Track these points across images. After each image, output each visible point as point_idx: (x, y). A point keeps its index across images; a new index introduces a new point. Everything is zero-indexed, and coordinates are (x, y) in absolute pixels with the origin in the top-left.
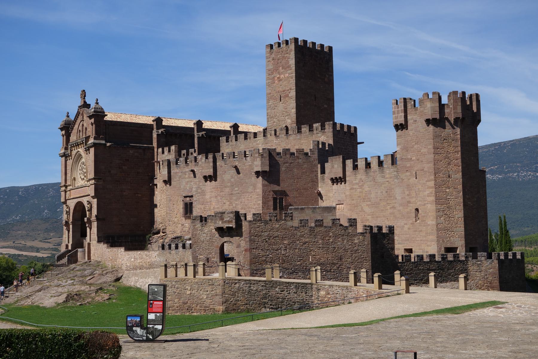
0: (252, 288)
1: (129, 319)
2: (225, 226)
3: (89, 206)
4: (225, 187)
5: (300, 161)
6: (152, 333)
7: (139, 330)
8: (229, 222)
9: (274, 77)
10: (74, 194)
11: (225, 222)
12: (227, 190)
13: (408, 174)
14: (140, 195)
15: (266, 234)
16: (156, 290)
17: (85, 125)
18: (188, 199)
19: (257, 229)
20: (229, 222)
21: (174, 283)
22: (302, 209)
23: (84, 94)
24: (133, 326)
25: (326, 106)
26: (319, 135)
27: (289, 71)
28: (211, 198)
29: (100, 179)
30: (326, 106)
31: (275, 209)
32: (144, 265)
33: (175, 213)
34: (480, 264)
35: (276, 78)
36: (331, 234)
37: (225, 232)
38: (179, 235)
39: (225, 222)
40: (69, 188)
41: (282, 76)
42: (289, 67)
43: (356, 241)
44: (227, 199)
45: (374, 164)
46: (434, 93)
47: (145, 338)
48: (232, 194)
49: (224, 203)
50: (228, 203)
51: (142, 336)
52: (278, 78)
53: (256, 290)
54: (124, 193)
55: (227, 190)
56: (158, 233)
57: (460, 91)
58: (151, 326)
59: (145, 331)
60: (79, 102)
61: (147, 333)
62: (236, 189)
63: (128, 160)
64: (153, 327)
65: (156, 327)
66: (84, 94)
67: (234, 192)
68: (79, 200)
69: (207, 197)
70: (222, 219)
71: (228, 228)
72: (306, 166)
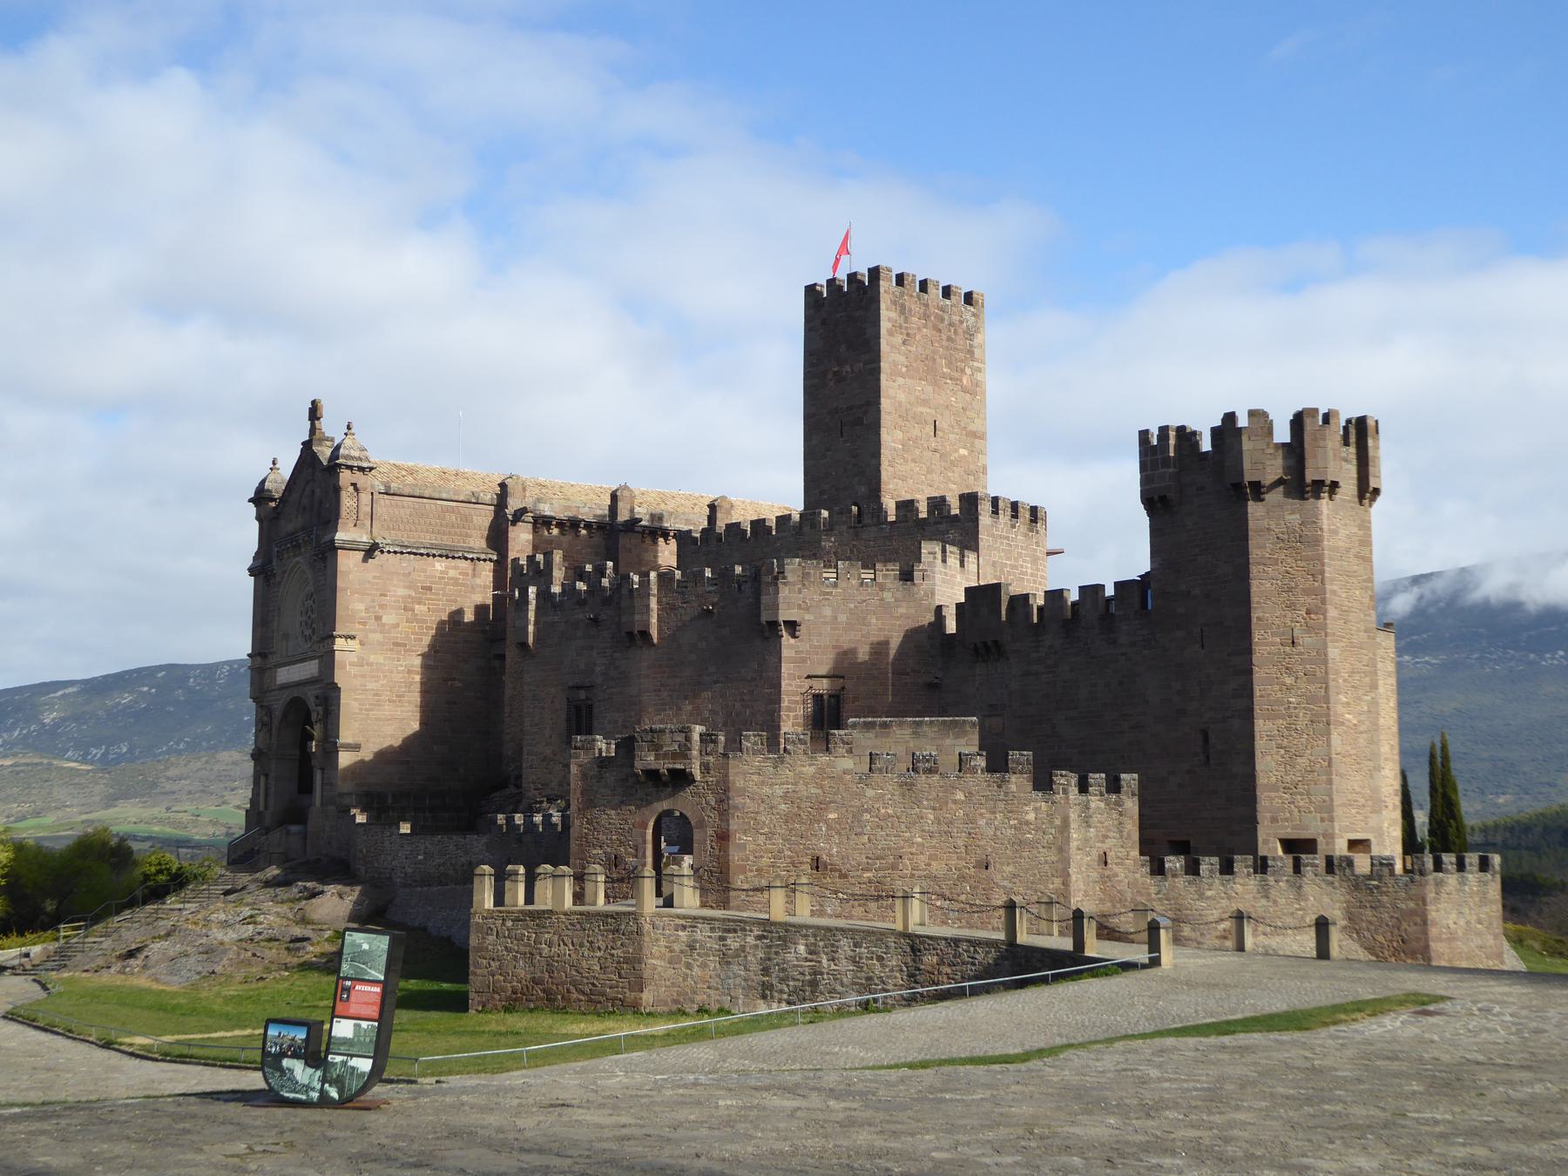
0: (729, 942)
1: (273, 1032)
2: (664, 766)
3: (320, 709)
5: (887, 596)
6: (338, 1082)
7: (299, 1070)
10: (285, 675)
11: (665, 755)
14: (458, 684)
15: (779, 791)
16: (366, 947)
17: (318, 491)
18: (582, 695)
19: (755, 778)
21: (509, 924)
22: (885, 725)
23: (314, 413)
24: (282, 1055)
25: (963, 452)
26: (943, 527)
29: (353, 638)
30: (963, 452)
34: (1377, 887)
35: (830, 376)
36: (960, 796)
37: (665, 785)
39: (665, 755)
40: (272, 660)
41: (848, 368)
43: (1031, 816)
46: (1252, 414)
47: (315, 1095)
51: (308, 1088)
53: (743, 948)
57: (1322, 411)
58: (338, 1059)
59: (319, 1073)
61: (324, 1080)
63: (430, 589)
64: (344, 1063)
65: (354, 1062)
66: (314, 413)
68: (296, 693)
70: (656, 748)
72: (902, 610)
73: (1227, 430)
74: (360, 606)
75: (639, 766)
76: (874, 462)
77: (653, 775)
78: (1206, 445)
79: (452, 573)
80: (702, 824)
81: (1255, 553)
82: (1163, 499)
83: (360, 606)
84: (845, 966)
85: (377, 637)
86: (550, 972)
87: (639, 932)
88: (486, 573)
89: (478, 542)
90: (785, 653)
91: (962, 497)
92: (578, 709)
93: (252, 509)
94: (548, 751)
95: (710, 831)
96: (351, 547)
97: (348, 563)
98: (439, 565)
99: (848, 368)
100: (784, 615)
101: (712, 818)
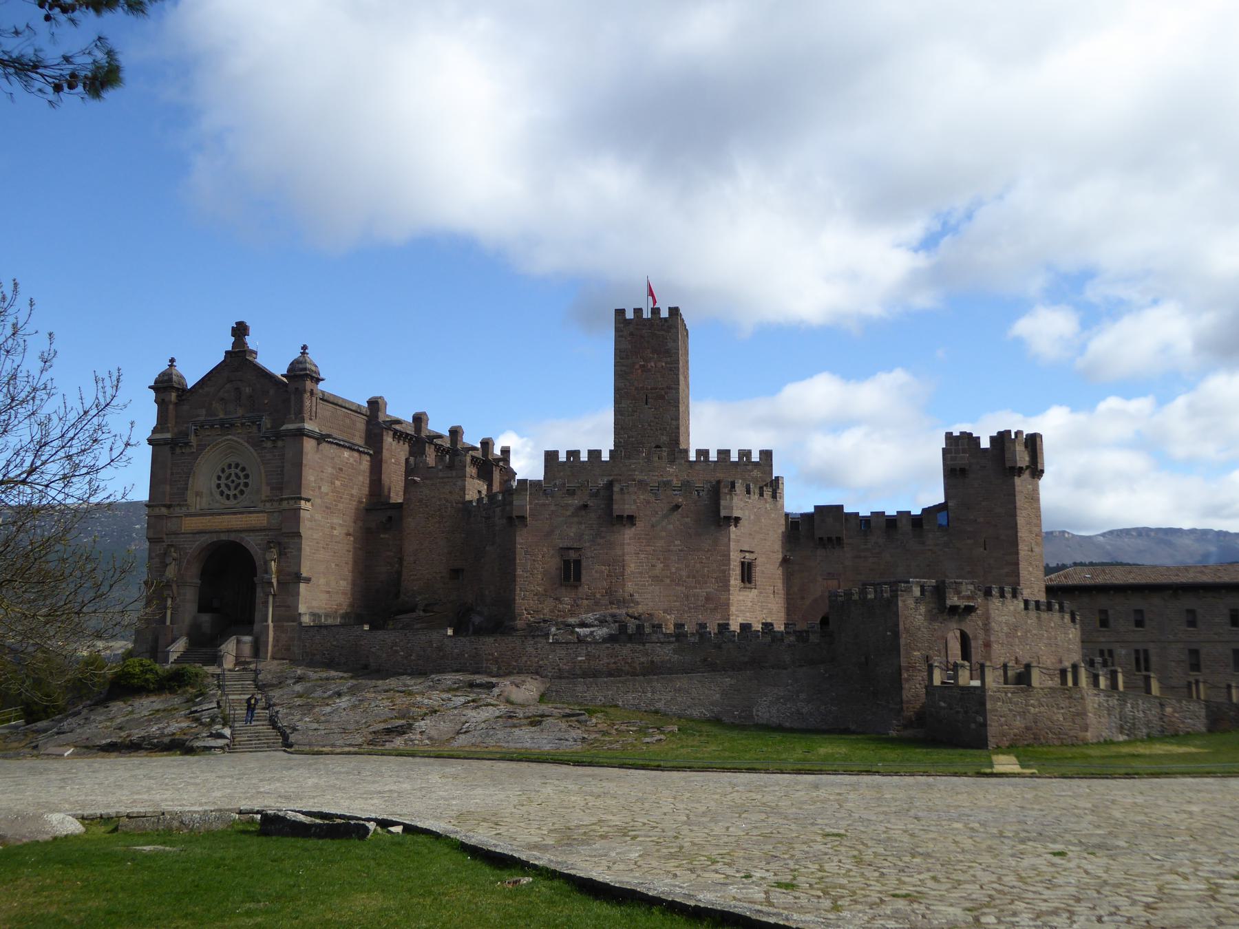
2: (963, 603)
8: (968, 598)
12: (660, 544)
13: (969, 541)
20: (968, 598)
26: (749, 467)
31: (743, 581)
32: (627, 668)
39: (963, 598)
45: (905, 526)
54: (335, 532)
55: (660, 543)
56: (413, 610)
60: (228, 343)
68: (224, 537)
70: (958, 593)
71: (966, 607)
73: (1001, 439)
74: (312, 479)
75: (949, 603)
76: (674, 423)
77: (954, 610)
78: (985, 443)
79: (351, 460)
80: (976, 638)
81: (1018, 504)
82: (963, 471)
83: (312, 479)
84: (1141, 715)
85: (318, 501)
86: (1035, 722)
87: (1082, 698)
88: (365, 462)
89: (359, 440)
90: (732, 536)
91: (761, 452)
92: (566, 563)
93: (152, 394)
95: (980, 642)
96: (311, 435)
97: (309, 445)
98: (346, 454)
100: (736, 514)
101: (981, 634)
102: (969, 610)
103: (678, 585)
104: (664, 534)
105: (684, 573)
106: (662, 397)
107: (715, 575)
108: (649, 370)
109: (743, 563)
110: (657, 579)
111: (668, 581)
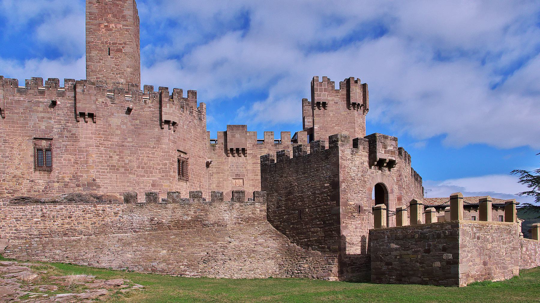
2: (388, 157)
4: (112, 135)
9: (99, 25)
12: (116, 139)
18: (44, 144)
27: (125, 23)
28: (87, 146)
33: (17, 161)
35: (102, 26)
38: (25, 196)
41: (113, 25)
42: (124, 17)
44: (115, 152)
48: (123, 146)
49: (111, 157)
50: (117, 157)
52: (106, 26)
62: (129, 140)
67: (126, 144)
69: (82, 144)
94: (18, 173)
99: (113, 25)
102: (391, 164)
103: (130, 173)
104: (119, 132)
105: (135, 164)
106: (120, 51)
107: (159, 167)
108: (111, 30)
109: (179, 161)
110: (113, 168)
111: (122, 170)
